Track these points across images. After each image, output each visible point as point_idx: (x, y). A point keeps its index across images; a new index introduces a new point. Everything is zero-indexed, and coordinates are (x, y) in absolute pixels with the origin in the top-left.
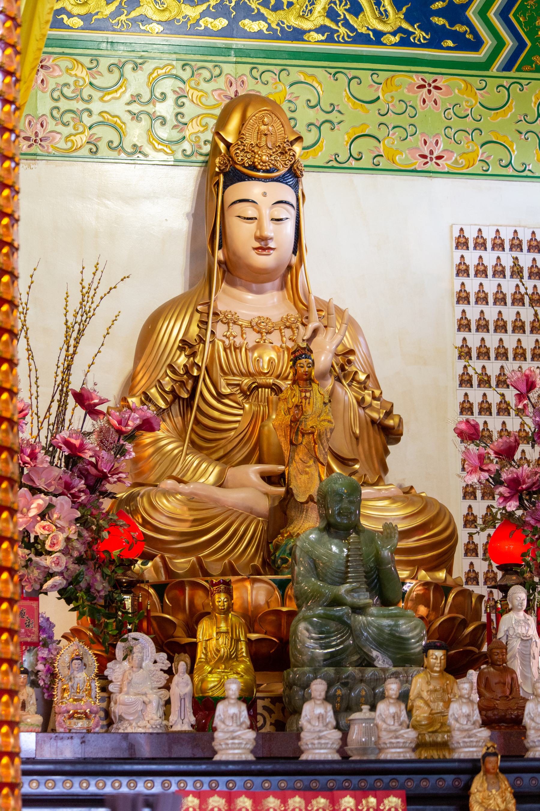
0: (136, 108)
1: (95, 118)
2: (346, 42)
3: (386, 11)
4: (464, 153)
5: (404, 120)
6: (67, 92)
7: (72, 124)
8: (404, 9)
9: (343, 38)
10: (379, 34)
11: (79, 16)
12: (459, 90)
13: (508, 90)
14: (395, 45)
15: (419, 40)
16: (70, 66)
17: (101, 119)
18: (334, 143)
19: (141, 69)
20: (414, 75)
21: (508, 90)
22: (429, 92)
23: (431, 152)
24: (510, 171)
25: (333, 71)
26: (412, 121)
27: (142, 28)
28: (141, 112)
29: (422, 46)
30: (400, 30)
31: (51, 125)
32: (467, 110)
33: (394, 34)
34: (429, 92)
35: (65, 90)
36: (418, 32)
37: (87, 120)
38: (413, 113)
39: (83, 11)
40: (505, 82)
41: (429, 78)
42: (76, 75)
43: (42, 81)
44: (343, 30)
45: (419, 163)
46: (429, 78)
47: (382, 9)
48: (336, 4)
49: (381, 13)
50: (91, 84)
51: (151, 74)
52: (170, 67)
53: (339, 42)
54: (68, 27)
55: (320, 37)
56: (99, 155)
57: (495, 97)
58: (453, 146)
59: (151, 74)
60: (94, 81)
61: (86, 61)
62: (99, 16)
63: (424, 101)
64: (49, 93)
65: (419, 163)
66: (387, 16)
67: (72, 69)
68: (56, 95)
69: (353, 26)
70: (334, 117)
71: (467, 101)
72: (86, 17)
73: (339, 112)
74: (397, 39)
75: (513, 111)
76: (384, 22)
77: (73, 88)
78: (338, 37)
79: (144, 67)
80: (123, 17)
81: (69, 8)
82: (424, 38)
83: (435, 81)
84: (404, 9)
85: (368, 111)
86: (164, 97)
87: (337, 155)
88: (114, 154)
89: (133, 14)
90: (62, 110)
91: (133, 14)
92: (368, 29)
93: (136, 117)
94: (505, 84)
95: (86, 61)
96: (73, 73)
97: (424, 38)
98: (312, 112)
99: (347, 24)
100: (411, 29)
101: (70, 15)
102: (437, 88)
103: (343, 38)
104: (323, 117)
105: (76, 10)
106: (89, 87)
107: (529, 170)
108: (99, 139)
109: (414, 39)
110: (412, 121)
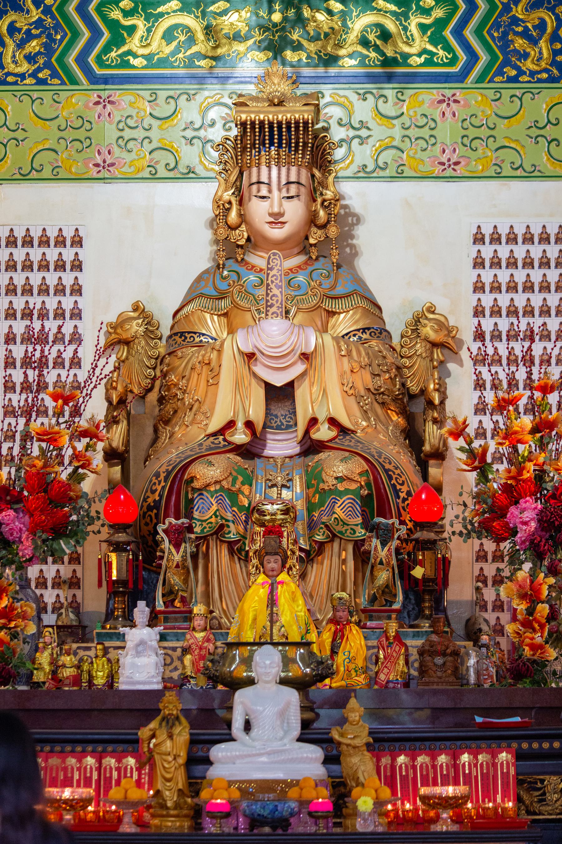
0: (189, 134)
1: (155, 145)
2: (376, 66)
3: (412, 35)
4: (479, 158)
5: (425, 133)
6: (131, 122)
7: (135, 150)
8: (429, 33)
9: (374, 62)
10: (406, 56)
11: (143, 56)
12: (476, 102)
13: (521, 99)
14: (421, 65)
15: (442, 60)
16: (133, 100)
17: (160, 145)
18: (363, 154)
19: (194, 99)
20: (435, 91)
21: (521, 99)
22: (448, 105)
23: (449, 160)
24: (519, 173)
25: (361, 92)
26: (433, 133)
27: (197, 63)
28: (194, 138)
29: (444, 65)
30: (424, 51)
31: (116, 151)
32: (482, 120)
33: (419, 55)
34: (448, 105)
35: (129, 121)
36: (441, 53)
37: (148, 147)
38: (433, 125)
39: (146, 51)
40: (518, 93)
41: (448, 93)
42: (138, 108)
43: (109, 115)
44: (373, 55)
45: (438, 170)
46: (448, 93)
47: (408, 34)
48: (367, 33)
49: (407, 37)
50: (151, 114)
51: (203, 103)
52: (219, 96)
53: (370, 66)
54: (133, 67)
55: (353, 62)
56: (157, 176)
57: (507, 108)
58: (470, 153)
59: (203, 103)
60: (154, 113)
61: (146, 94)
62: (161, 55)
63: (444, 113)
64: (115, 124)
65: (438, 170)
66: (413, 40)
67: (134, 103)
68: (121, 126)
69: (382, 51)
70: (364, 133)
71: (483, 111)
72: (148, 57)
73: (368, 128)
74: (422, 59)
75: (525, 118)
76: (411, 46)
77: (135, 118)
78: (369, 61)
79: (197, 97)
80: (181, 55)
81: (135, 49)
82: (447, 58)
83: (454, 95)
84: (429, 33)
85: (394, 126)
86: (213, 124)
87: (365, 166)
88: (171, 174)
89: (188, 53)
90: (126, 139)
91: (188, 53)
92: (396, 52)
93: (190, 142)
94: (518, 94)
95: (146, 94)
96: (136, 105)
97: (447, 58)
98: (343, 129)
99: (377, 48)
100: (434, 50)
101: (135, 56)
102: (456, 101)
103: (374, 62)
104: (352, 133)
105: (141, 51)
106: (149, 117)
107: (539, 171)
108: (157, 162)
109: (437, 58)
110: (433, 133)
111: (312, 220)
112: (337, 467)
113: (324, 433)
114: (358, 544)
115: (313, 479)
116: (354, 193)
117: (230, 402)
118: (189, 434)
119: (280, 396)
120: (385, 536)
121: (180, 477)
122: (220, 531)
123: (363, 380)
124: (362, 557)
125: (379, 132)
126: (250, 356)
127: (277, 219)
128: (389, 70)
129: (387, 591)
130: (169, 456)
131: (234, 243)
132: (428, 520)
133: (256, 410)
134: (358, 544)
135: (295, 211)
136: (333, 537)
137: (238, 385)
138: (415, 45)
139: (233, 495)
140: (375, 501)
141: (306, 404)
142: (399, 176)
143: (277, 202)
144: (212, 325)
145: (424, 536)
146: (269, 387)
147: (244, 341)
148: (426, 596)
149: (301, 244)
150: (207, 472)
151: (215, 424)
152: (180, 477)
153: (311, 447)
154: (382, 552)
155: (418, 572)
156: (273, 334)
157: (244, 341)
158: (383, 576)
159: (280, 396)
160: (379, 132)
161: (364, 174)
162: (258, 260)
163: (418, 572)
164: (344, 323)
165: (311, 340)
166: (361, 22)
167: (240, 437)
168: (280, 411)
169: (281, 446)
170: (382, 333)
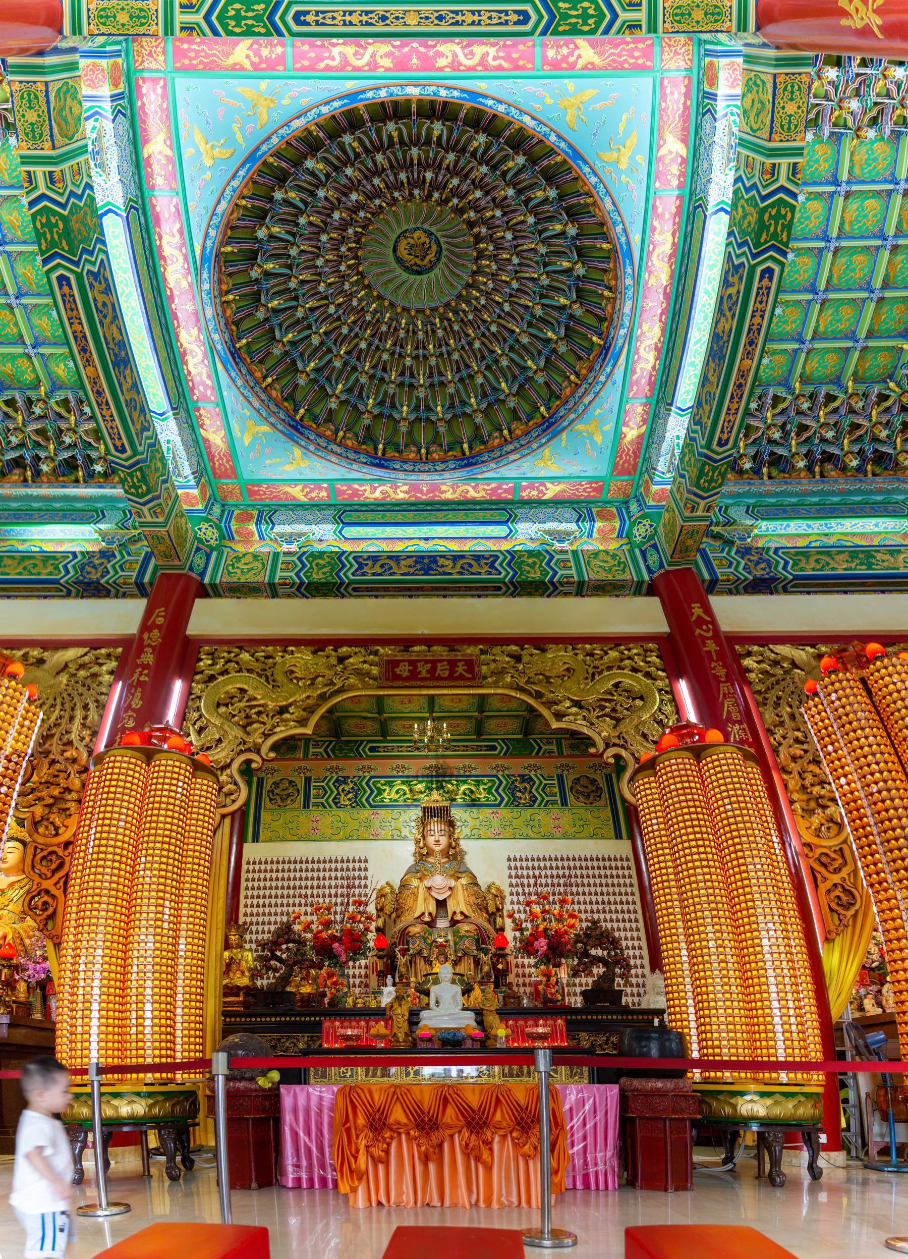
18: (466, 831)
111: (450, 846)
112: (465, 928)
113: (459, 917)
114: (475, 957)
115: (456, 934)
116: (464, 844)
117: (423, 906)
118: (407, 919)
119: (441, 904)
120: (486, 953)
121: (404, 933)
122: (420, 952)
123: (473, 899)
124: (477, 962)
125: (472, 823)
126: (429, 889)
127: (437, 842)
128: (474, 804)
129: (488, 974)
130: (400, 925)
131: (423, 855)
132: (502, 945)
133: (432, 908)
134: (475, 957)
135: (444, 841)
136: (465, 954)
137: (425, 899)
138: (482, 795)
139: (425, 939)
140: (481, 939)
141: (451, 907)
142: (480, 838)
143: (437, 837)
144: (415, 883)
145: (500, 955)
146: (437, 901)
147: (427, 883)
148: (500, 977)
149: (445, 853)
150: (416, 929)
151: (417, 914)
152: (404, 933)
153: (454, 923)
154: (484, 958)
155: (500, 966)
156: (438, 881)
157: (427, 883)
158: (486, 968)
159: (441, 904)
160: (472, 823)
161: (468, 838)
162: (431, 860)
163: (500, 966)
164: (464, 881)
165: (452, 883)
166: (463, 788)
167: (427, 918)
168: (442, 912)
169: (442, 924)
170: (477, 884)
